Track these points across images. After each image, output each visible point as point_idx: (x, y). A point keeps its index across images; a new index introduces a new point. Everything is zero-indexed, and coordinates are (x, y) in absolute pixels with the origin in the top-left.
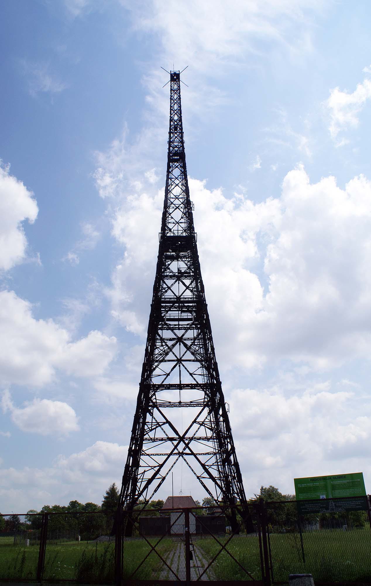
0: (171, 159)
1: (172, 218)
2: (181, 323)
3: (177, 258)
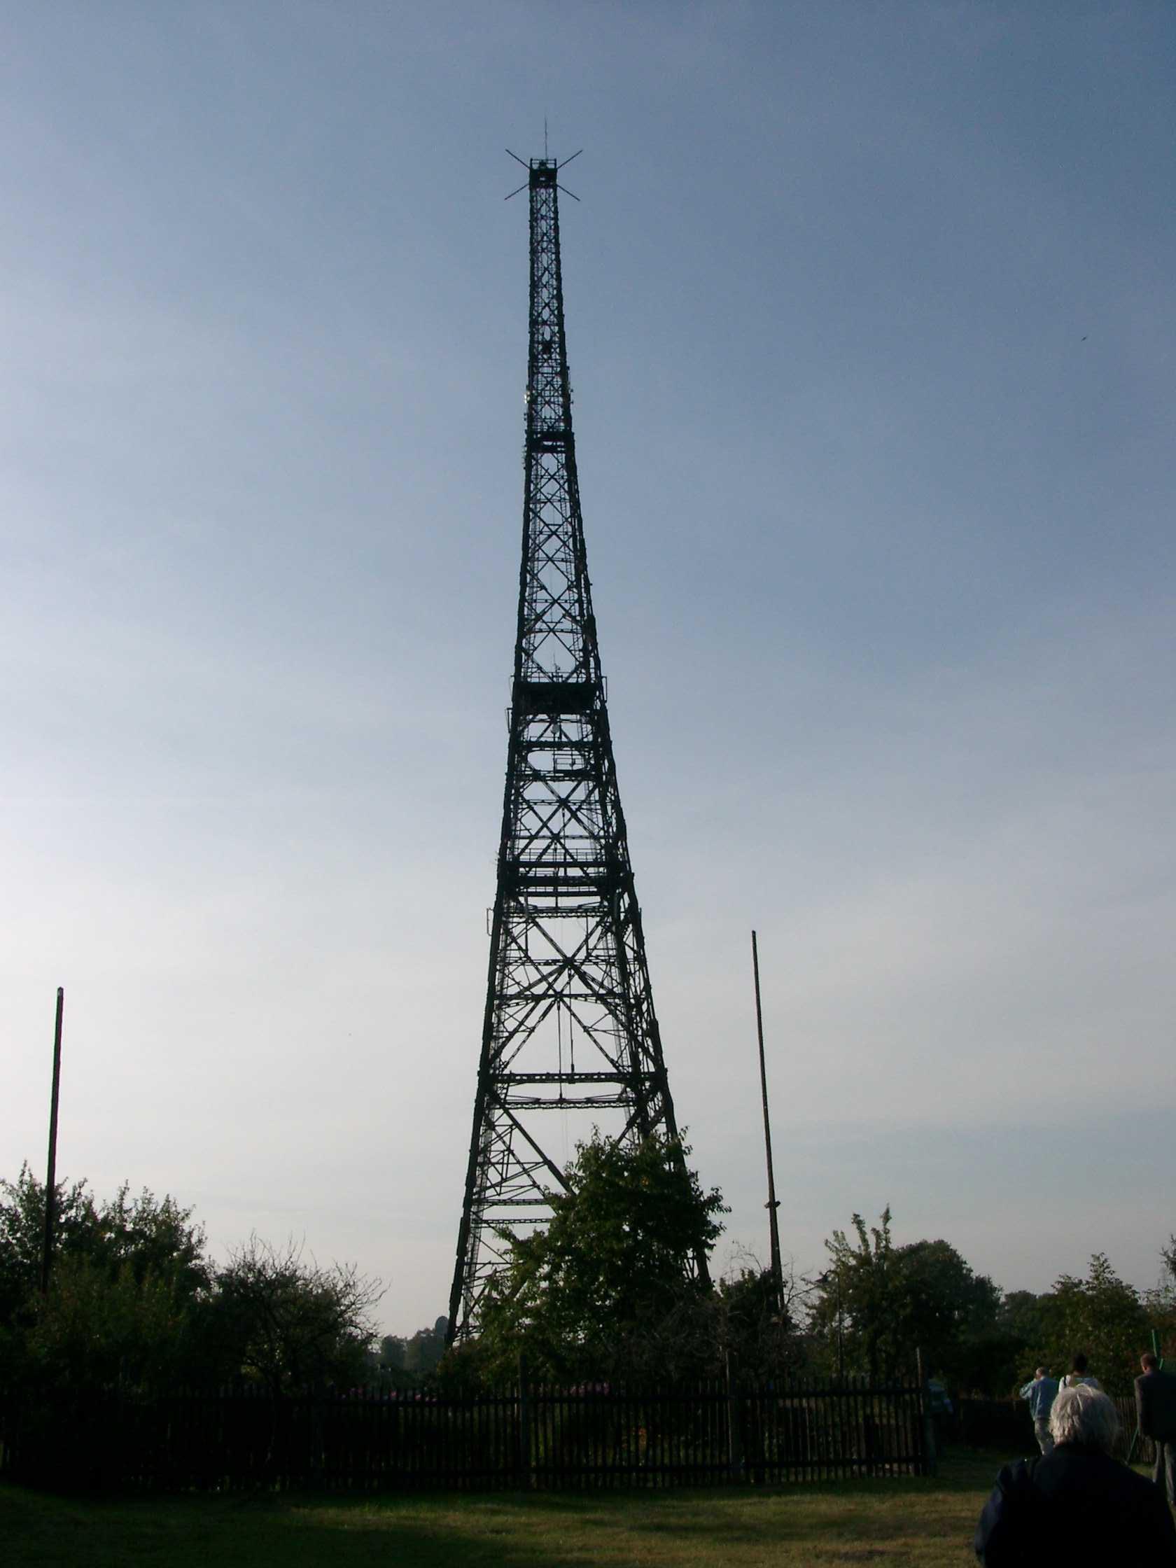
0: (536, 443)
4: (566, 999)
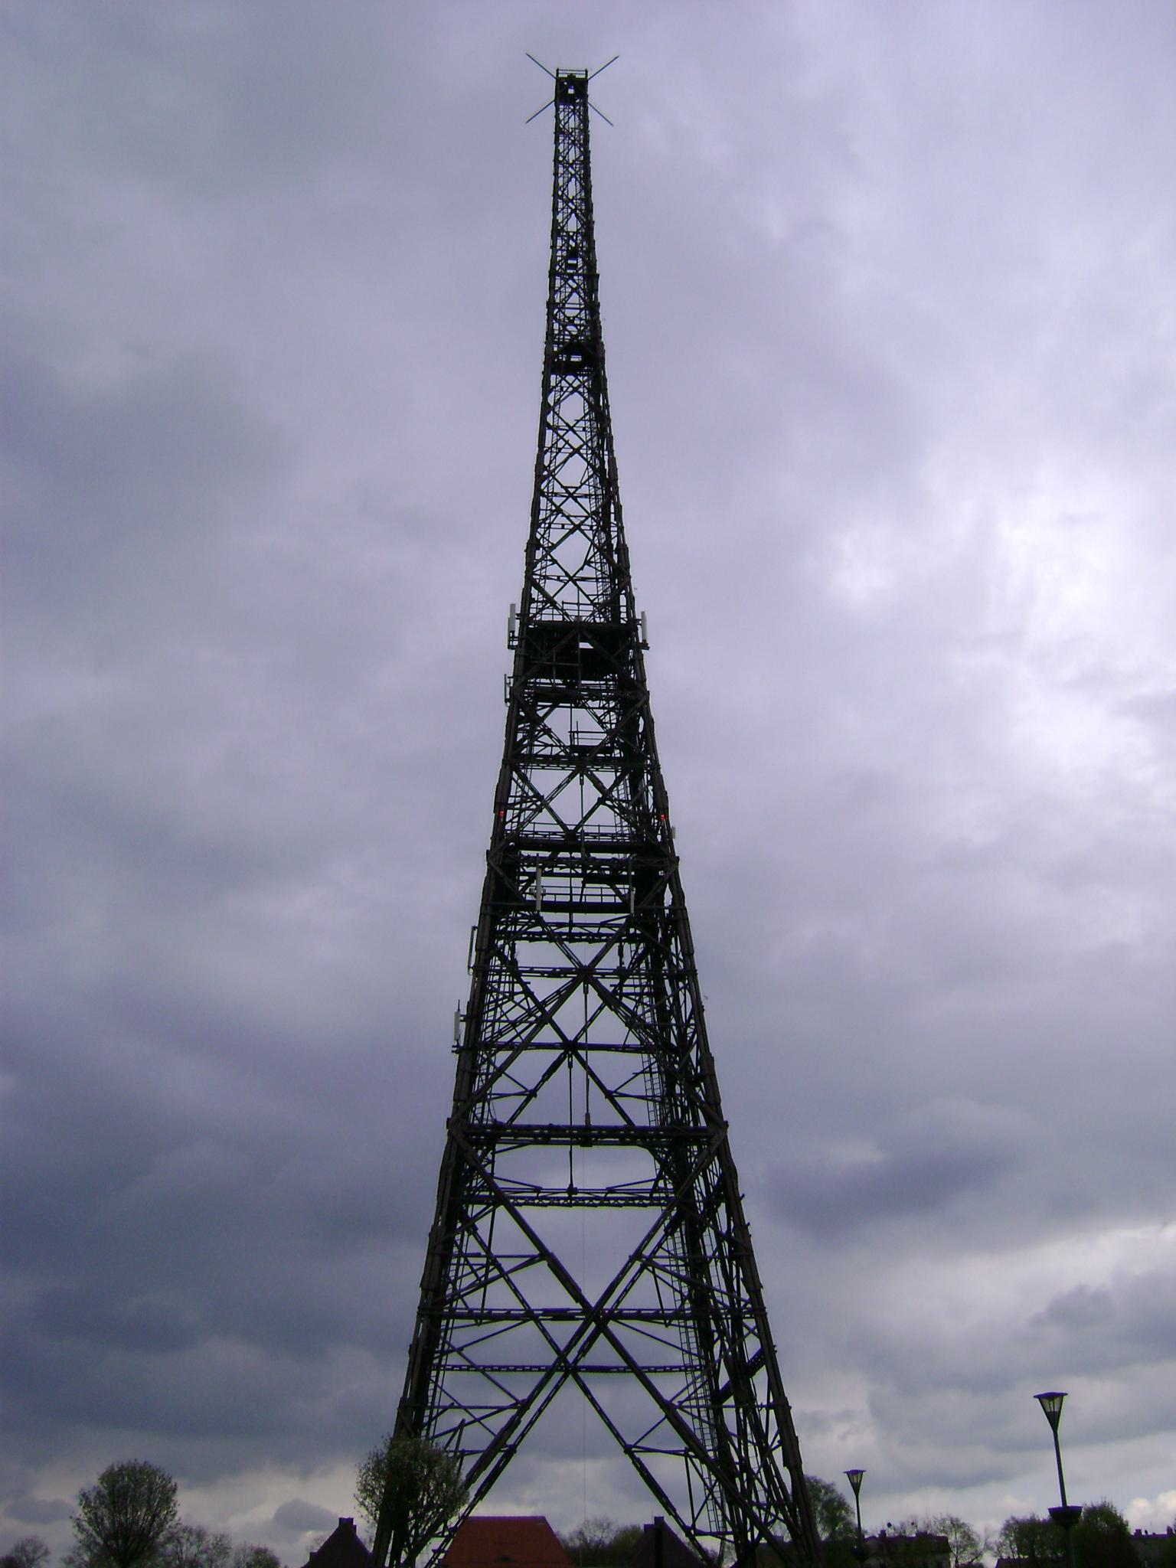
1: (554, 561)
2: (578, 918)
3: (574, 698)
4: (582, 1053)
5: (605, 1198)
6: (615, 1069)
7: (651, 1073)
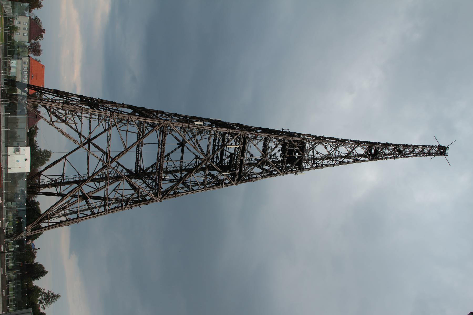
5: (139, 153)
6: (176, 156)
7: (174, 167)
